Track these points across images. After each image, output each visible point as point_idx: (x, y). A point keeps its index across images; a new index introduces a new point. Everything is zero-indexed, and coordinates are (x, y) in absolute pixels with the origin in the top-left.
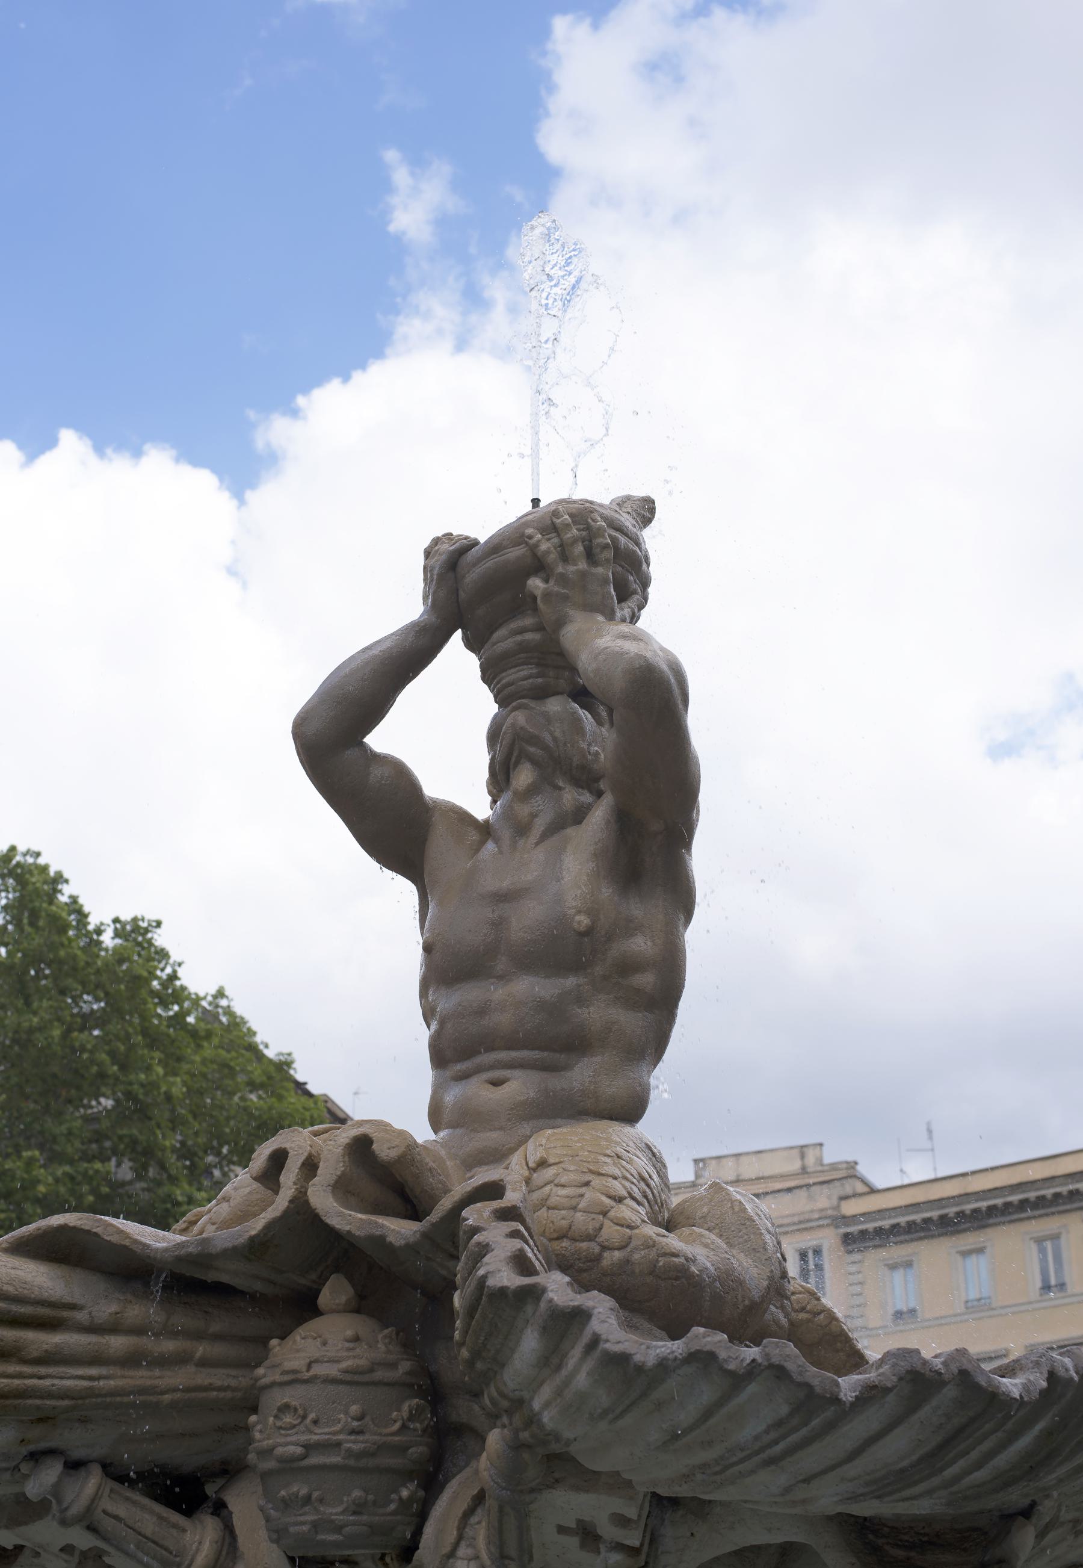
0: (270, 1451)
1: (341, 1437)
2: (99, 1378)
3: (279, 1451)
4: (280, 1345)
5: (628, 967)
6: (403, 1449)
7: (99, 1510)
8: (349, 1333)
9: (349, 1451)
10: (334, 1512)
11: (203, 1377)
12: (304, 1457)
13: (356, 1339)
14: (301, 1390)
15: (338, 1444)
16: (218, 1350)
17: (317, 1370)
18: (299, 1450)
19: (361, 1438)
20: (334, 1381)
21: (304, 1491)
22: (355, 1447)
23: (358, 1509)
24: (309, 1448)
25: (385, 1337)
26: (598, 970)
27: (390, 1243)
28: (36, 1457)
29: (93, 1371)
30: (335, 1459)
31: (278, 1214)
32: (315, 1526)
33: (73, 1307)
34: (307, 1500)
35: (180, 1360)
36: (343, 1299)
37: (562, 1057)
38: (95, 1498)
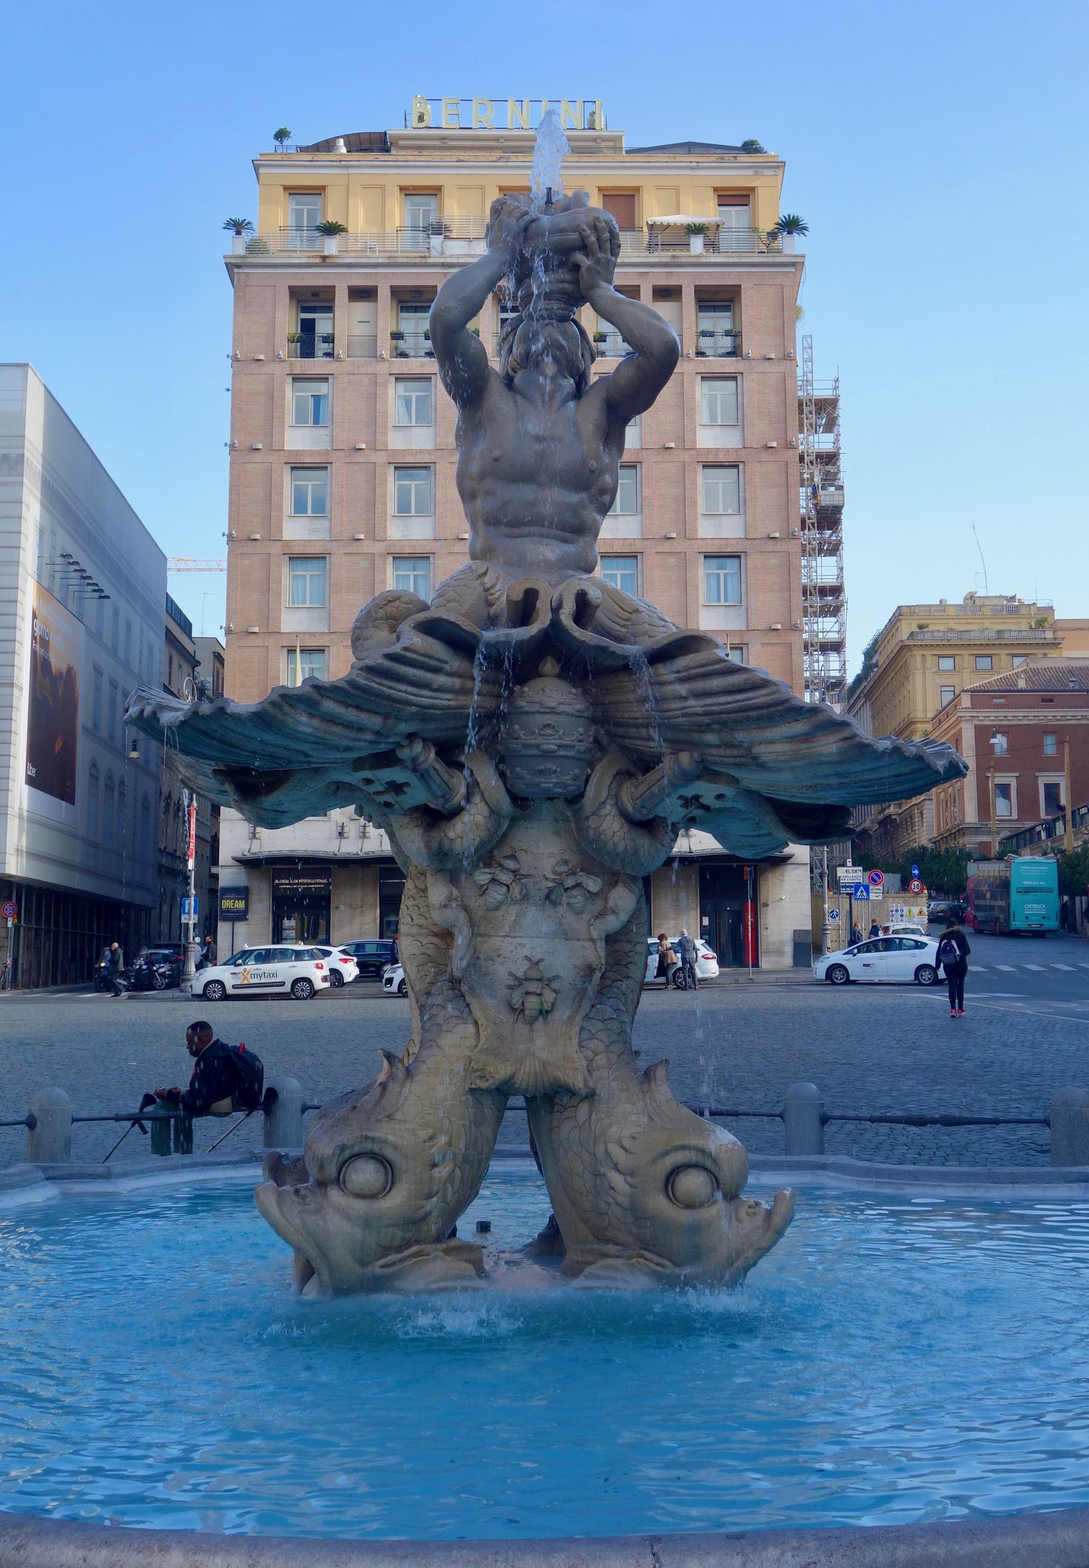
5: (603, 491)
9: (579, 751)
10: (567, 779)
14: (554, 717)
15: (574, 747)
21: (554, 768)
22: (583, 749)
23: (576, 778)
24: (560, 746)
26: (593, 491)
28: (411, 737)
30: (571, 753)
32: (556, 784)
37: (567, 535)
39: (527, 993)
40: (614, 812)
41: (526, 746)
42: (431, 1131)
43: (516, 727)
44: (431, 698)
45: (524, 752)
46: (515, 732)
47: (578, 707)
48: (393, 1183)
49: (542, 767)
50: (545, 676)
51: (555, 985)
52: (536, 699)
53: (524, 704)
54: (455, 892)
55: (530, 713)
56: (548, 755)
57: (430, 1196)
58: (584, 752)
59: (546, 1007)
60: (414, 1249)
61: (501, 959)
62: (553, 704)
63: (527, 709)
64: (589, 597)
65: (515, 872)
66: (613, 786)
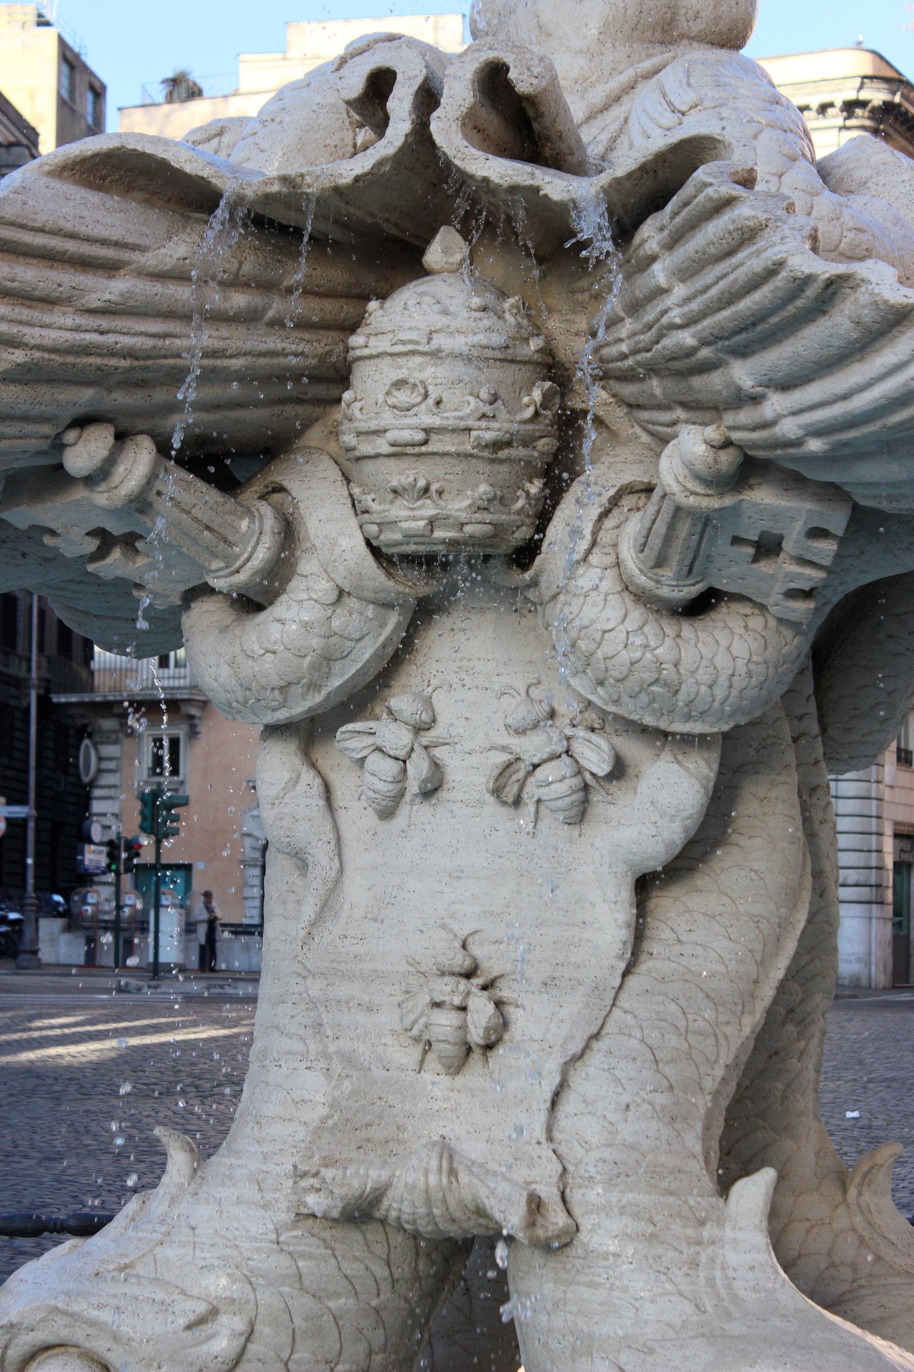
0: (379, 432)
1: (470, 423)
2: (164, 336)
3: (391, 436)
4: (382, 307)
6: (528, 442)
7: (155, 490)
8: (476, 301)
11: (273, 342)
12: (426, 442)
13: (484, 309)
16: (297, 306)
18: (420, 436)
19: (495, 425)
21: (422, 483)
22: (489, 436)
25: (512, 306)
27: (546, 196)
28: (82, 422)
29: (155, 327)
31: (391, 151)
32: (432, 523)
33: (134, 248)
35: (248, 318)
36: (458, 257)
38: (152, 478)
39: (437, 1005)
40: (609, 583)
42: (202, 1308)
44: (77, 329)
45: (366, 448)
51: (504, 992)
52: (386, 324)
58: (497, 446)
59: (476, 1036)
64: (512, 75)
65: (419, 729)
66: (609, 523)
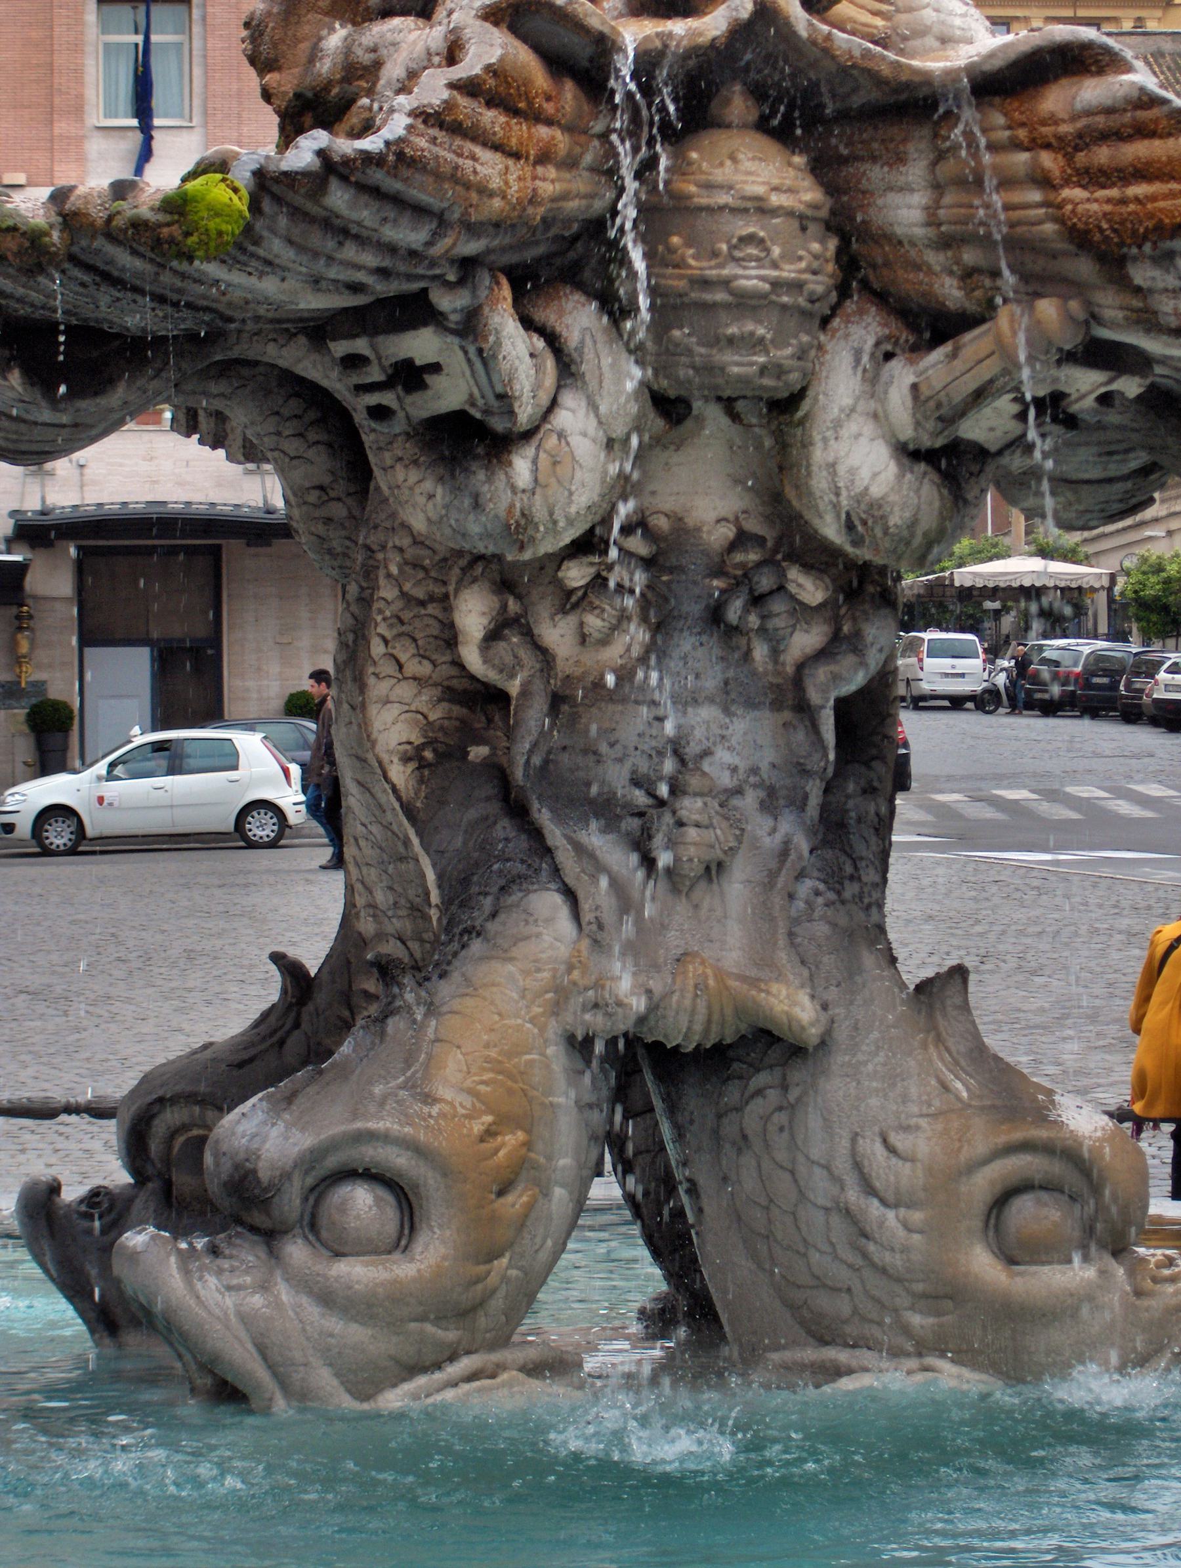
15: (796, 286)
17: (776, 200)
20: (790, 213)
24: (776, 284)
32: (763, 370)
34: (762, 340)
41: (705, 283)
43: (675, 240)
46: (671, 250)
47: (808, 197)
48: (412, 1228)
49: (733, 330)
50: (728, 126)
53: (693, 189)
54: (513, 606)
55: (709, 209)
56: (746, 304)
57: (493, 1255)
60: (465, 1364)
61: (618, 751)
62: (760, 190)
63: (704, 201)
